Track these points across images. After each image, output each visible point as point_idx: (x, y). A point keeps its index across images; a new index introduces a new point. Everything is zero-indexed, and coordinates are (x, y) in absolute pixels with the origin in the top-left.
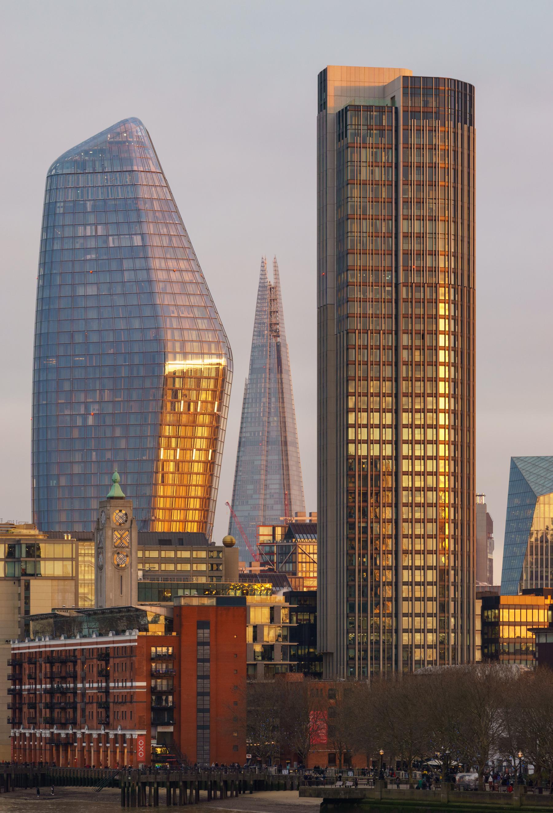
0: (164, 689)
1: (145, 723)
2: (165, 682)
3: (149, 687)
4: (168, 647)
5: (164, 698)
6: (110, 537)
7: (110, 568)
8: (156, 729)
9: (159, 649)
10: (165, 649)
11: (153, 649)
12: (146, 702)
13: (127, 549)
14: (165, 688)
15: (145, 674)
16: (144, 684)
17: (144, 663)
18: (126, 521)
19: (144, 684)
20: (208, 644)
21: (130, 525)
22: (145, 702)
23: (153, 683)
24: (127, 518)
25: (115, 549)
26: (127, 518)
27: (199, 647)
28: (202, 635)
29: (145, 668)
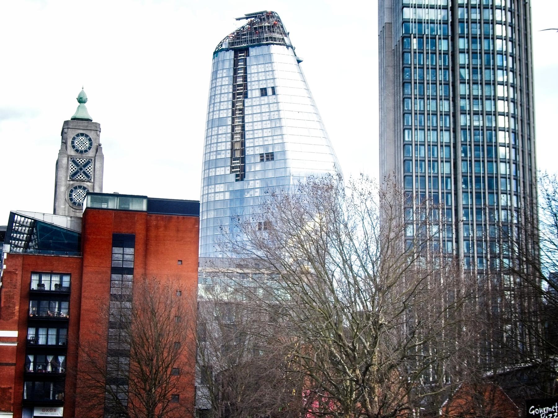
0: (50, 343)
1: (12, 402)
2: (53, 332)
3: (23, 341)
4: (62, 275)
5: (50, 359)
6: (65, 166)
7: (63, 207)
8: (32, 412)
9: (45, 279)
10: (56, 279)
11: (35, 278)
12: (15, 364)
13: (88, 183)
14: (52, 342)
15: (16, 318)
16: (14, 334)
17: (17, 299)
18: (90, 148)
19: (14, 334)
20: (130, 271)
21: (94, 153)
22: (12, 365)
23: (31, 333)
24: (91, 144)
25: (72, 182)
26: (91, 144)
27: (114, 276)
28: (121, 256)
29: (17, 308)
